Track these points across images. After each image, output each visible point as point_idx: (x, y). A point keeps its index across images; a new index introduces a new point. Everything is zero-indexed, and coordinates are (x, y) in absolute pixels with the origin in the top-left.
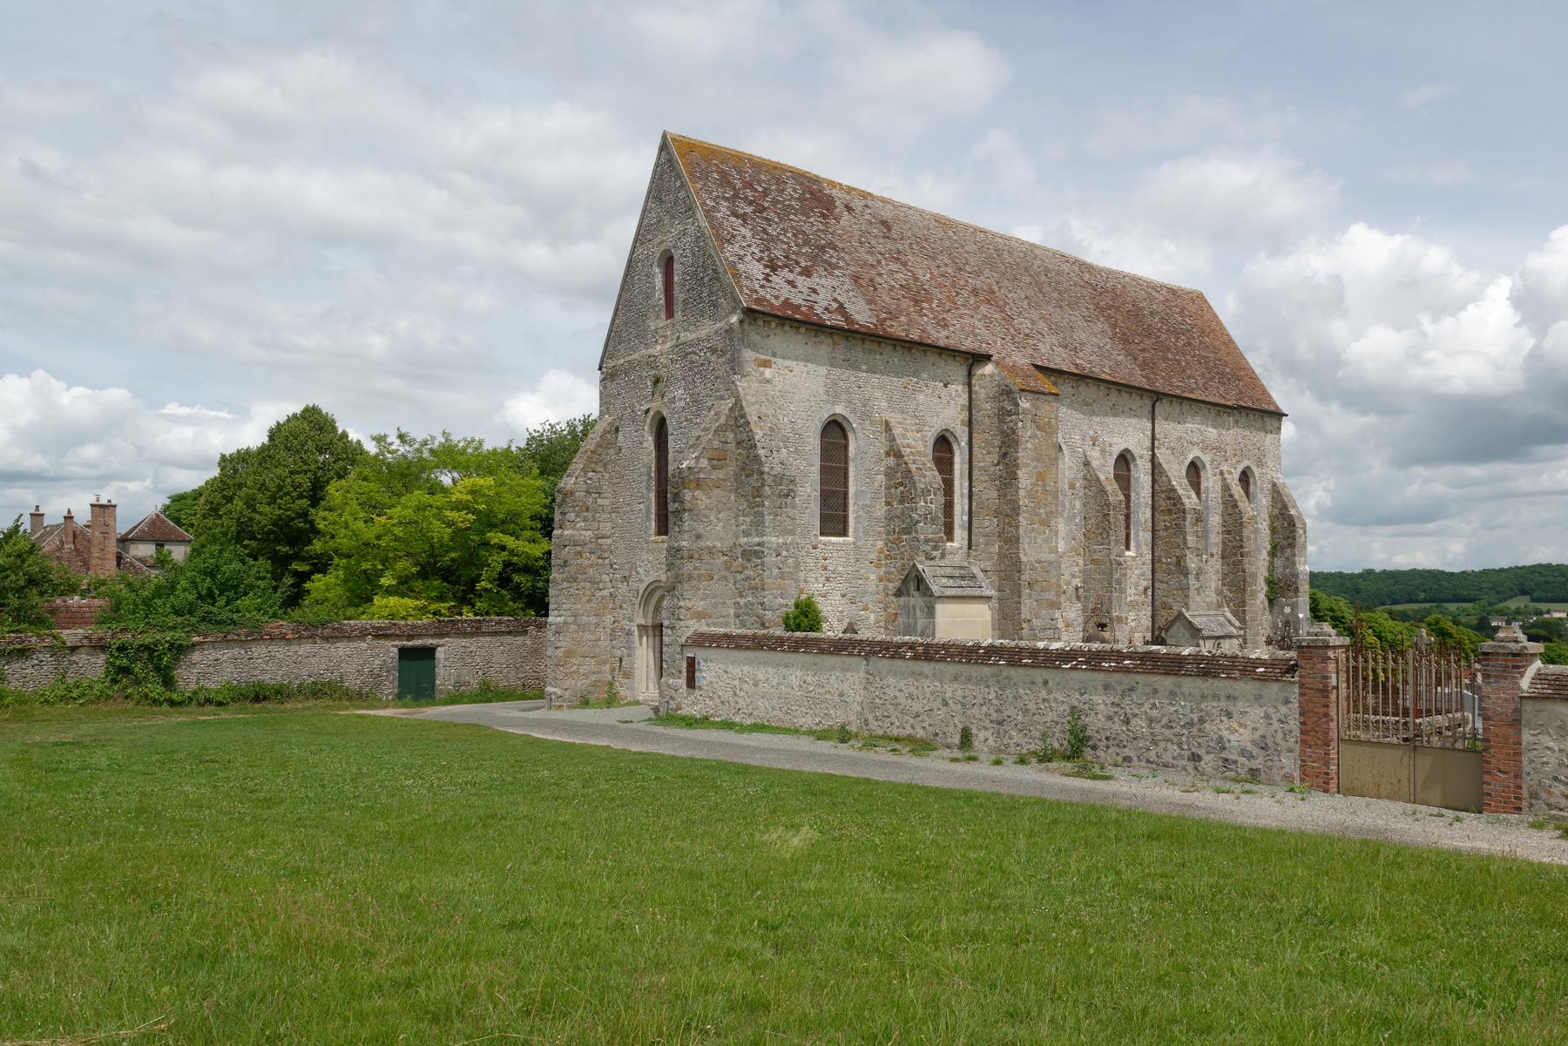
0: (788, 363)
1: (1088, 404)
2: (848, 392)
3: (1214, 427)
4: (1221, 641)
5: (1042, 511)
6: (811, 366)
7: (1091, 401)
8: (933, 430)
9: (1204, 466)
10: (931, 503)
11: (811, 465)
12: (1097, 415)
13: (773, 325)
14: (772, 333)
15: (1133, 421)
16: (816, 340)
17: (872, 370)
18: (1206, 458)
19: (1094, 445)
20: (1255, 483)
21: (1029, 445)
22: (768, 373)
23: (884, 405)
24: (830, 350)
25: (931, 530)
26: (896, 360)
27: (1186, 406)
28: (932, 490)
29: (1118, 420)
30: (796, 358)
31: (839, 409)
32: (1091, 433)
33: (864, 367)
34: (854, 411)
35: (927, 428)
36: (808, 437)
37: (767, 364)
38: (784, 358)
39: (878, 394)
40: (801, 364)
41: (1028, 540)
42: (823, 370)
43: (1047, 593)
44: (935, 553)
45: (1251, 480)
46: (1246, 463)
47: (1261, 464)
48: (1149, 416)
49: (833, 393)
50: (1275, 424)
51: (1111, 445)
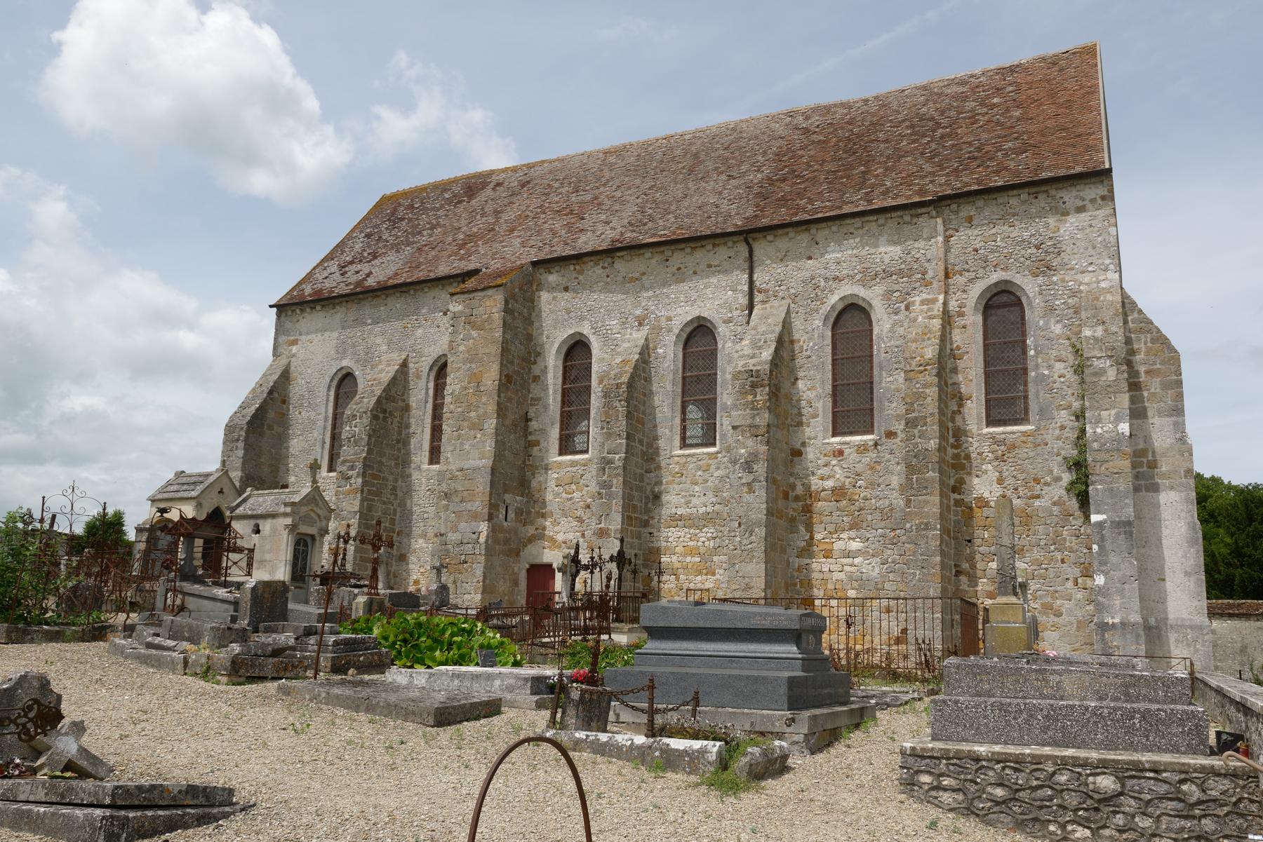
0: (310, 337)
1: (632, 280)
2: (354, 346)
3: (895, 243)
4: (261, 522)
5: (473, 414)
6: (327, 334)
7: (637, 275)
8: (429, 358)
9: (870, 305)
10: (355, 427)
11: (319, 414)
12: (647, 290)
13: (298, 311)
14: (301, 318)
15: (714, 280)
16: (332, 311)
17: (375, 322)
18: (873, 296)
19: (640, 324)
20: (1030, 304)
21: (462, 348)
22: (294, 349)
23: (385, 348)
24: (343, 316)
25: (352, 452)
26: (398, 306)
27: (822, 233)
28: (358, 414)
29: (684, 286)
30: (317, 331)
31: (345, 363)
32: (638, 312)
33: (369, 321)
34: (357, 361)
35: (423, 359)
36: (319, 392)
37: (295, 342)
38: (308, 334)
39: (379, 340)
40: (319, 335)
41: (451, 448)
42: (335, 334)
43: (469, 504)
44: (350, 473)
45: (1024, 300)
46: (995, 277)
47: (1044, 268)
48: (746, 265)
49: (342, 351)
50: (1102, 191)
51: (669, 319)
